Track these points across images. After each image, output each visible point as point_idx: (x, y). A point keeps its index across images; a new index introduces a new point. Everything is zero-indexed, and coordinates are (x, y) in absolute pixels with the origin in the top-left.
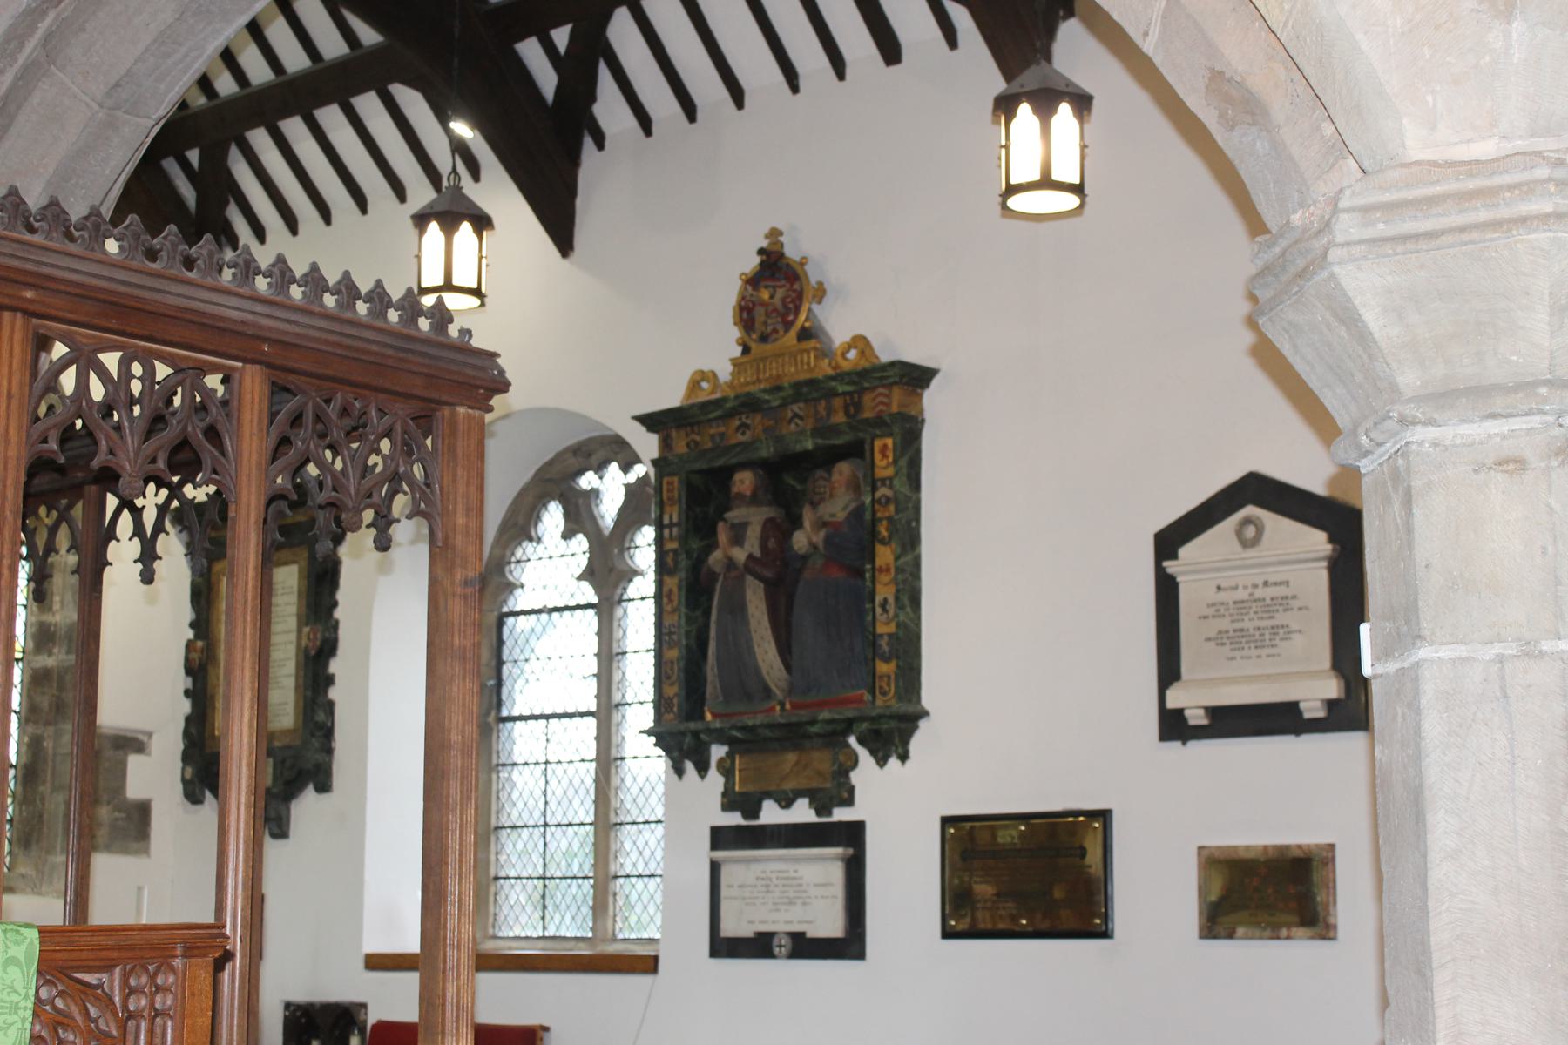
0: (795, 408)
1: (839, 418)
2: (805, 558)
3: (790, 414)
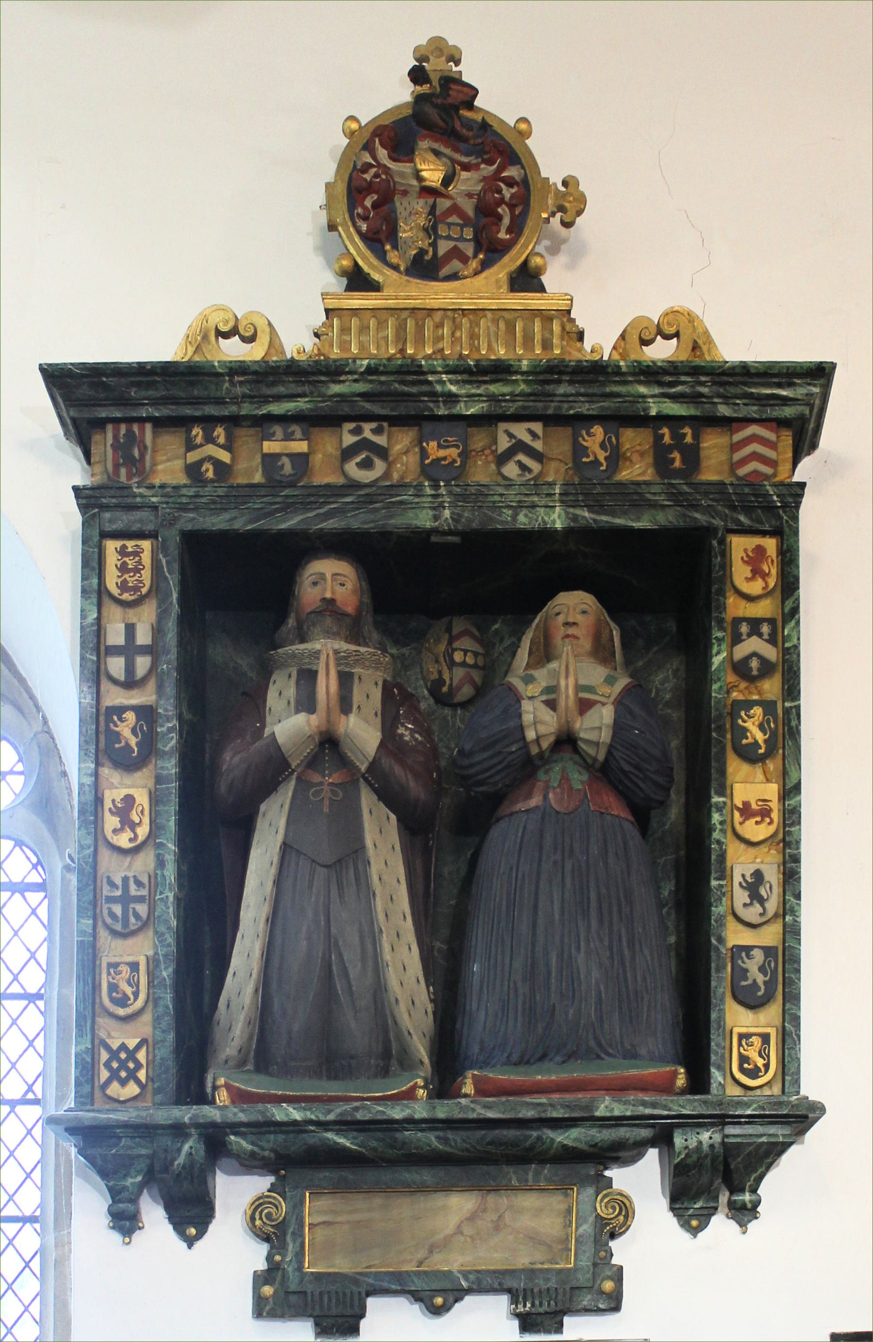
0: (520, 431)
1: (637, 470)
2: (528, 766)
3: (504, 443)
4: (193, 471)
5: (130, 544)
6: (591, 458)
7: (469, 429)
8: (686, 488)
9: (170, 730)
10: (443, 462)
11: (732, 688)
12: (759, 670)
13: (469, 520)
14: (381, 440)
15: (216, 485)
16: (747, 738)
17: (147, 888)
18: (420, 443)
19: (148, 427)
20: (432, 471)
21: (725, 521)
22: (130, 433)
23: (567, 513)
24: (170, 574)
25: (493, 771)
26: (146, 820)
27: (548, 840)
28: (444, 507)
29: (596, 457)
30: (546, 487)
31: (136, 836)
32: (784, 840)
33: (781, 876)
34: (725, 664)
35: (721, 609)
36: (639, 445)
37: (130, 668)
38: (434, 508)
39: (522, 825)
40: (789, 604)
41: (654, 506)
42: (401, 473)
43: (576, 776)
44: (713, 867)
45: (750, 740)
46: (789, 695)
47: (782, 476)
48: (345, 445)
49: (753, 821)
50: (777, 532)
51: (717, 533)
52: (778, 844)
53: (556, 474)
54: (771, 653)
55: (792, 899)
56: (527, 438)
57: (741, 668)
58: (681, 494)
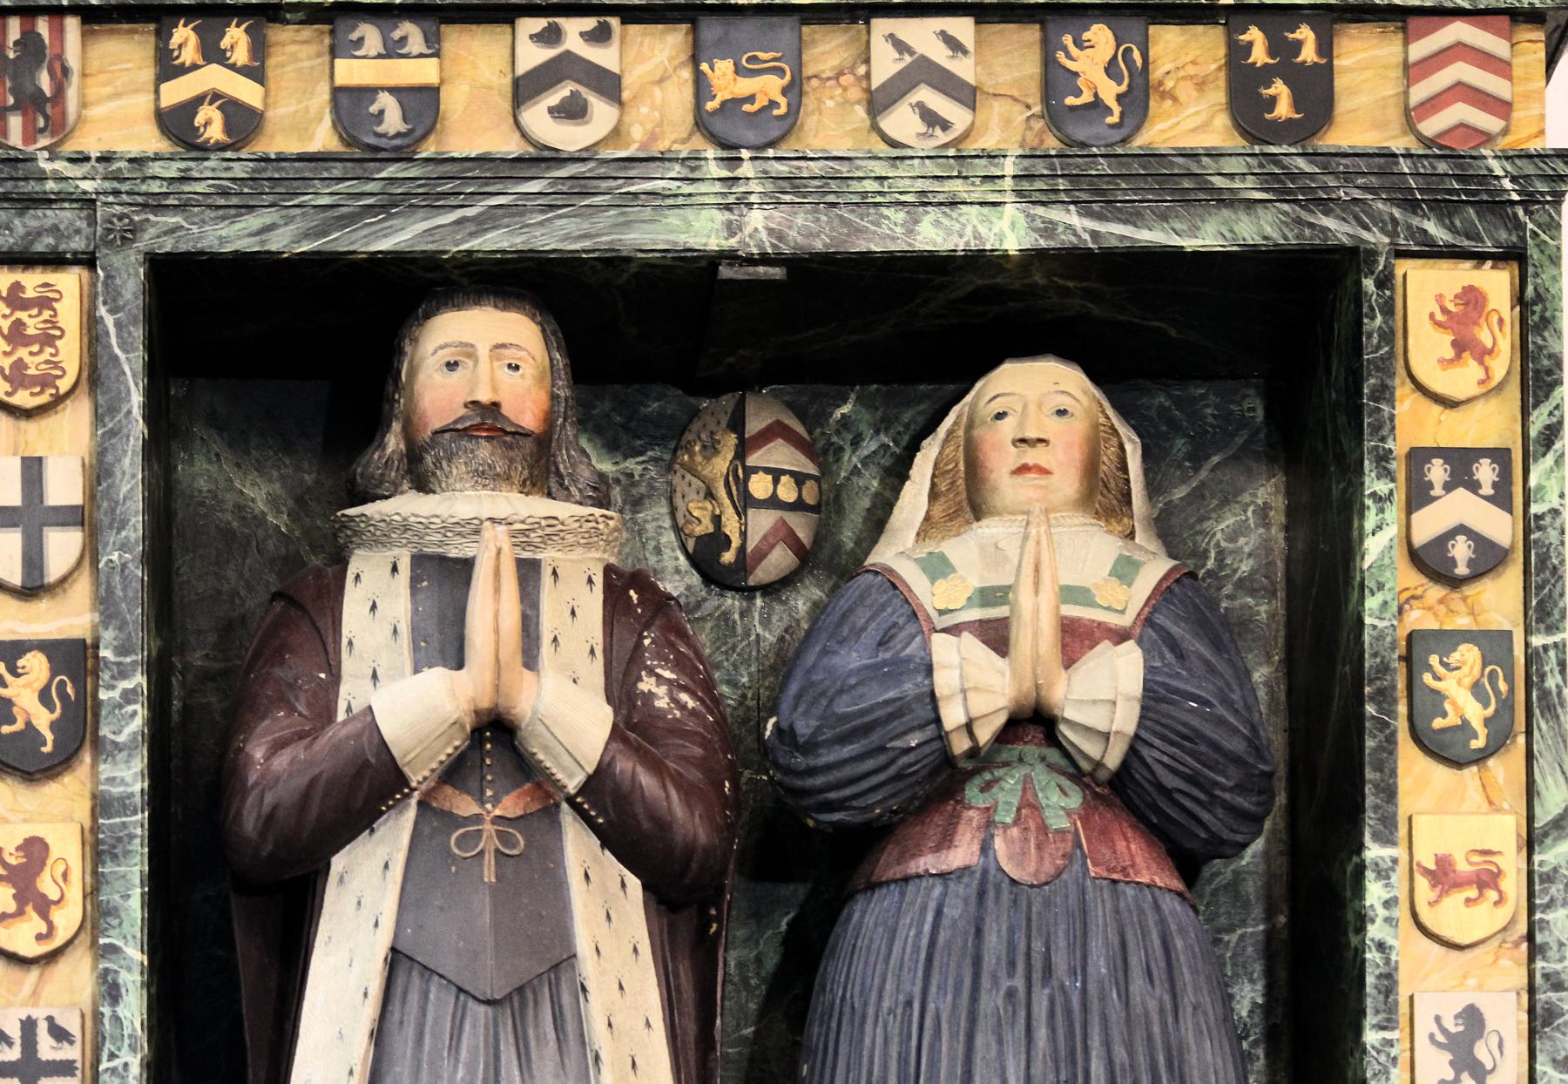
0: (923, 34)
3: (886, 64)
4: (176, 123)
5: (32, 281)
6: (1087, 97)
7: (805, 29)
8: (1302, 164)
9: (129, 697)
10: (747, 107)
11: (1407, 601)
12: (1471, 563)
13: (810, 235)
14: (604, 57)
15: (229, 154)
16: (1444, 715)
17: (78, 1044)
18: (695, 60)
19: (72, 24)
20: (719, 126)
21: (1393, 234)
22: (30, 41)
23: (1031, 218)
24: (126, 351)
25: (865, 785)
26: (75, 893)
27: (994, 942)
28: (750, 205)
29: (1096, 95)
30: (983, 162)
31: (51, 927)
32: (1530, 937)
33: (1525, 1017)
34: (1395, 552)
35: (1385, 432)
36: (1194, 63)
37: (33, 559)
38: (728, 207)
39: (932, 905)
40: (1540, 419)
41: (1227, 201)
42: (649, 126)
43: (1055, 797)
44: (1369, 1002)
45: (1452, 720)
46: (1539, 620)
47: (1521, 137)
48: (523, 67)
49: (1457, 898)
50: (1514, 255)
51: (1376, 262)
52: (1517, 945)
53: (1007, 130)
54: (1500, 527)
55: (1551, 1071)
56: (939, 54)
57: (1429, 561)
58: (1293, 176)
